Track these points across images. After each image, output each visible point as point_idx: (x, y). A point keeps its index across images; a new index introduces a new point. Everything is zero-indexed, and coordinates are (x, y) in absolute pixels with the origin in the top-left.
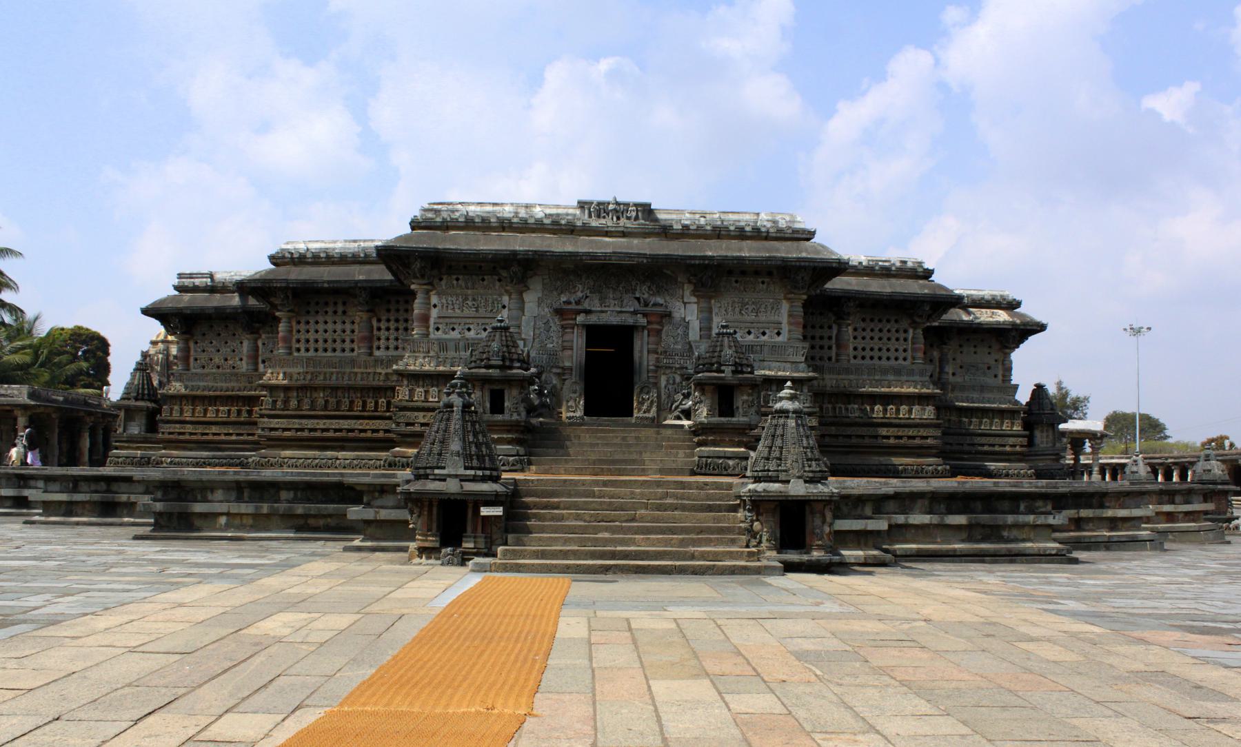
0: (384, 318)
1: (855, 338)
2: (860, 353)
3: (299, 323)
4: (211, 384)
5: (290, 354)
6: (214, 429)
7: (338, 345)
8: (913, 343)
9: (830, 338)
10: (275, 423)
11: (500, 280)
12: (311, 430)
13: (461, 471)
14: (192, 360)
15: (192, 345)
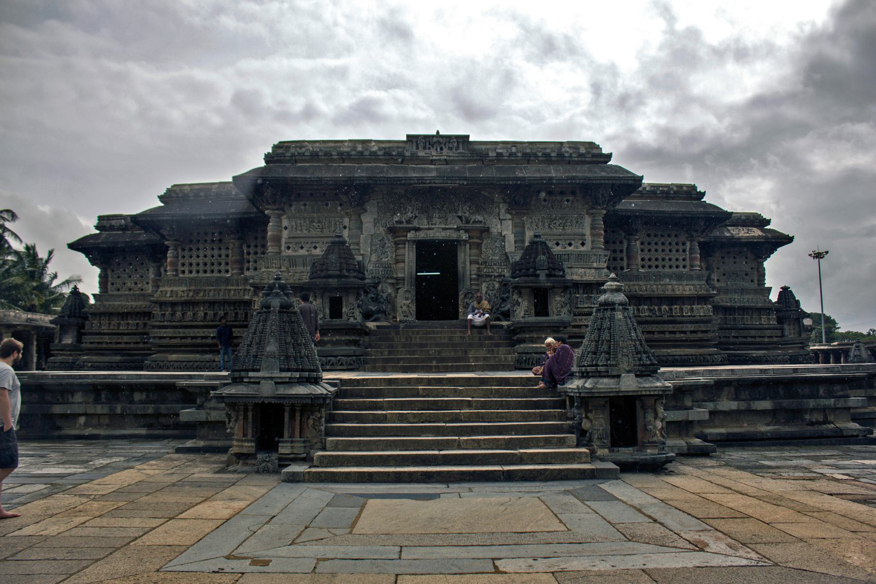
0: (252, 244)
1: (642, 250)
2: (647, 263)
3: (183, 250)
4: (124, 303)
5: (177, 275)
6: (126, 339)
7: (216, 268)
8: (691, 254)
9: (621, 251)
10: (163, 332)
11: (341, 205)
12: (193, 338)
13: (277, 374)
14: (109, 284)
15: (109, 272)
